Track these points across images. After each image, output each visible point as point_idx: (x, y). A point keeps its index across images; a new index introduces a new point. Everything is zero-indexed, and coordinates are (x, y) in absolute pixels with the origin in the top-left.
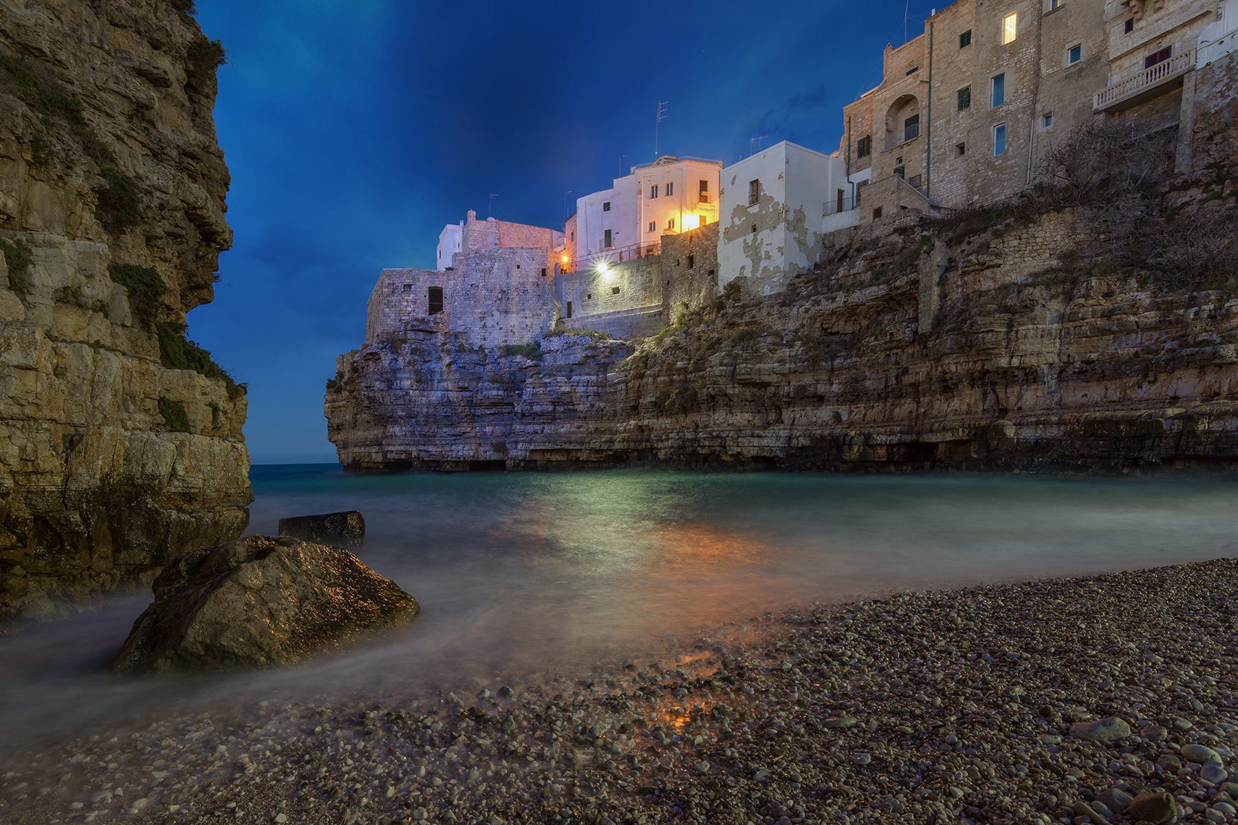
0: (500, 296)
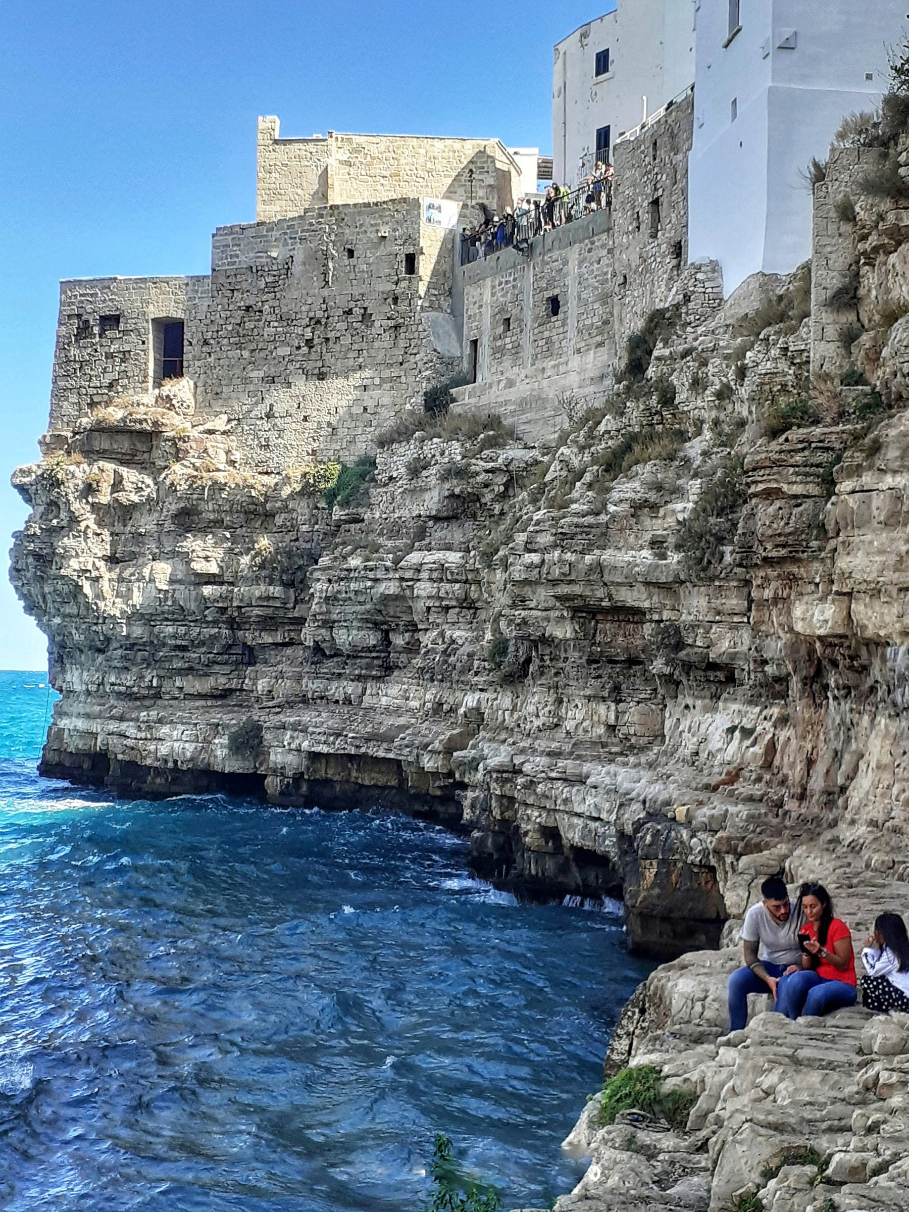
0: (309, 335)
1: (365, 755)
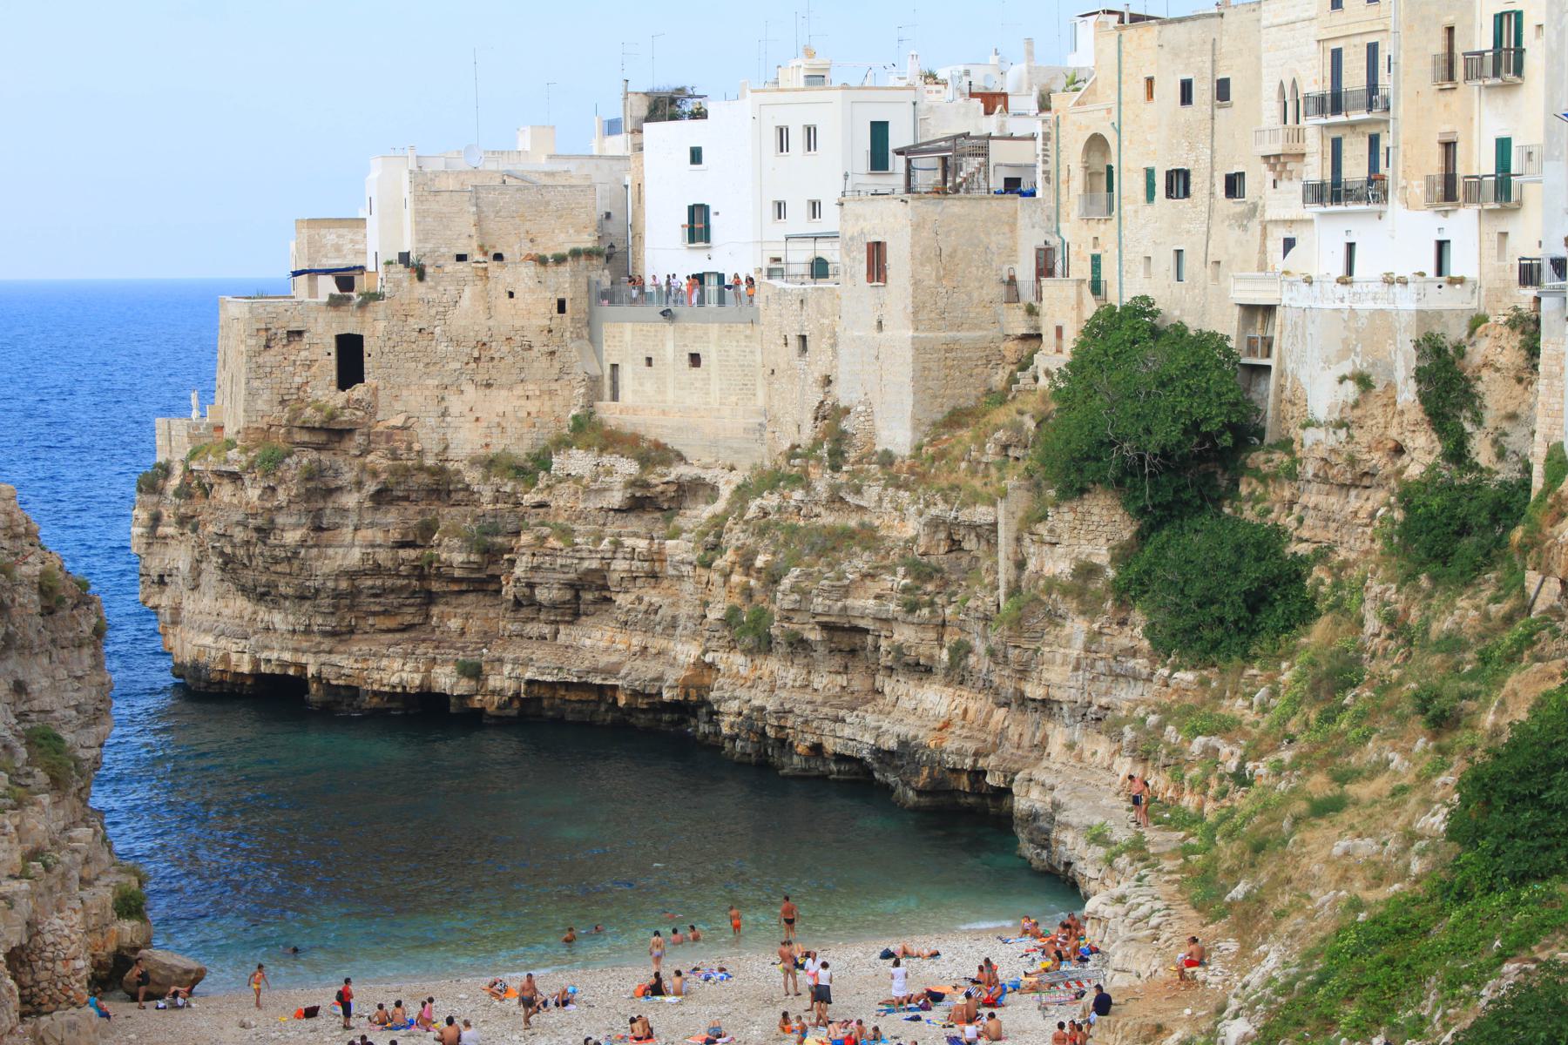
0: (476, 354)
1: (586, 683)
